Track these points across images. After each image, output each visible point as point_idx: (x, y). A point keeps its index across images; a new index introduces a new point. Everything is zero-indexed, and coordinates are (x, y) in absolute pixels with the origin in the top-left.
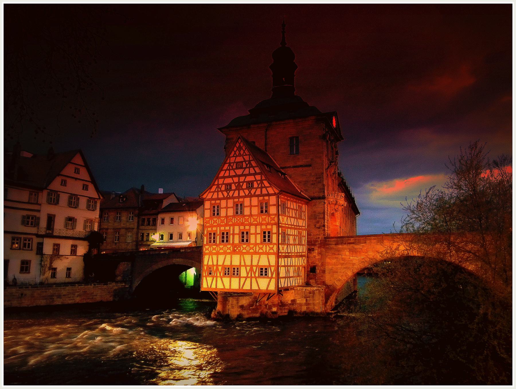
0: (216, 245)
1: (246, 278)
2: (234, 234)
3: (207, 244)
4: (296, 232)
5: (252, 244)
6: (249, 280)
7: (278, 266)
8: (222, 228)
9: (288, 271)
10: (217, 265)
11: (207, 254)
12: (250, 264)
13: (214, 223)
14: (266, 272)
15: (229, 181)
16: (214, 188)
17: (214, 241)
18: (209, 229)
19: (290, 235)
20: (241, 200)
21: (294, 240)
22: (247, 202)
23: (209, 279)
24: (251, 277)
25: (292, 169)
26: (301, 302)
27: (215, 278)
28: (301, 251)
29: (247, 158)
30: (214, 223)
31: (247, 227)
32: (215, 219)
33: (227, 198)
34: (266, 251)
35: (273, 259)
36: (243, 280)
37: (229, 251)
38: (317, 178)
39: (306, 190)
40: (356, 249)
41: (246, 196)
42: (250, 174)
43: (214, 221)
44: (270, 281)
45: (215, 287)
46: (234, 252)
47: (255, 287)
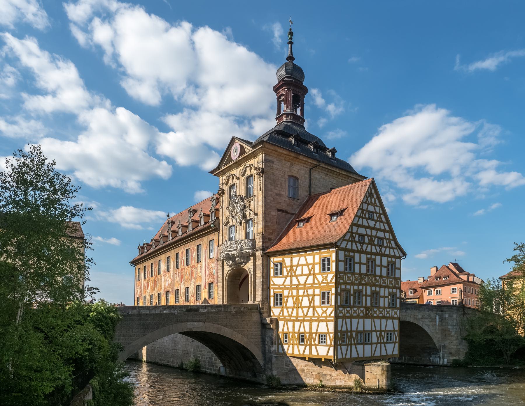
0: (350, 306)
2: (366, 295)
3: (341, 306)
5: (381, 308)
6: (379, 345)
8: (356, 287)
10: (351, 331)
12: (379, 329)
13: (348, 280)
15: (362, 231)
17: (346, 303)
18: (343, 287)
20: (373, 257)
23: (344, 348)
24: (381, 343)
27: (349, 346)
30: (348, 280)
31: (378, 289)
32: (349, 275)
36: (374, 346)
41: (377, 254)
42: (380, 230)
43: (348, 277)
46: (366, 316)
47: (384, 353)
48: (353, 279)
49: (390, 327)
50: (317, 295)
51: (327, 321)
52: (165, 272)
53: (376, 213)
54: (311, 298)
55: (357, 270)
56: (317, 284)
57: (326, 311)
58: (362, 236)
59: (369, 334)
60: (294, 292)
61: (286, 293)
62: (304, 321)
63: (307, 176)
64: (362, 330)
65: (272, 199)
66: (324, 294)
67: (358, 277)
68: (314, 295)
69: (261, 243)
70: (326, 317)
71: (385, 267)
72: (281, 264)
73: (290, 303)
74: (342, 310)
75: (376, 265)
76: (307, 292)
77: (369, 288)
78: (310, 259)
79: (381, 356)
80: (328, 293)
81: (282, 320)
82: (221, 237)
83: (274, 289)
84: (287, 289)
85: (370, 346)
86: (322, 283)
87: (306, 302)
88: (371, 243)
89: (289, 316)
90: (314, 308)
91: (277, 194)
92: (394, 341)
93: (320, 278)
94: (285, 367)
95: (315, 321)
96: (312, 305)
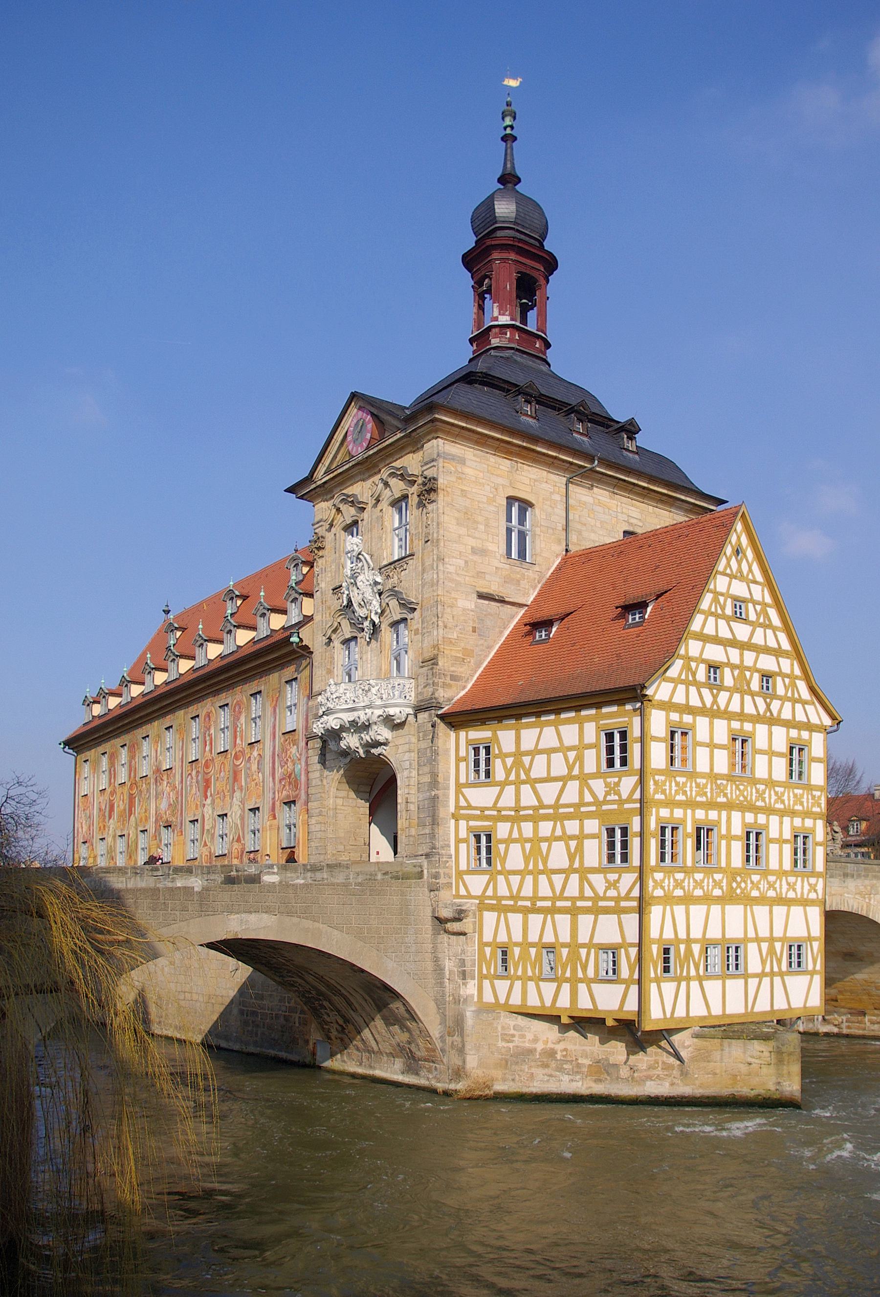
6: (766, 981)
8: (700, 814)
10: (689, 941)
11: (659, 900)
12: (767, 935)
14: (799, 956)
18: (664, 813)
23: (668, 988)
24: (772, 974)
31: (762, 819)
34: (802, 893)
36: (753, 983)
37: (717, 892)
43: (677, 784)
45: (684, 1015)
47: (780, 1004)
48: (692, 790)
49: (797, 930)
50: (593, 836)
51: (619, 911)
52: (158, 770)
53: (755, 603)
54: (573, 844)
55: (702, 766)
56: (589, 804)
57: (618, 881)
58: (714, 667)
59: (737, 948)
60: (527, 828)
61: (502, 830)
62: (553, 911)
63: (557, 497)
64: (720, 937)
65: (461, 563)
66: (611, 832)
67: (705, 786)
68: (581, 837)
69: (431, 690)
70: (618, 899)
71: (780, 755)
72: (488, 749)
73: (515, 858)
74: (663, 881)
76: (563, 827)
77: (736, 816)
78: (570, 733)
79: (772, 1011)
80: (625, 831)
81: (491, 908)
82: (318, 672)
83: (468, 818)
84: (506, 819)
85: (741, 982)
86: (605, 802)
87: (558, 856)
88: (742, 688)
89: (511, 897)
90: (584, 873)
91: (474, 551)
92: (810, 967)
93: (598, 786)
94: (501, 1044)
95: (587, 911)
96: (576, 865)
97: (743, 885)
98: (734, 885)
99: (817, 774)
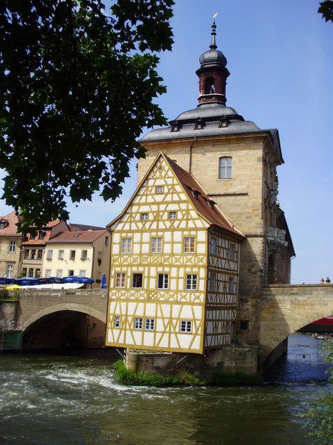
0: (126, 289)
1: (163, 333)
2: (149, 277)
4: (226, 278)
5: (173, 291)
6: (166, 336)
7: (206, 320)
9: (216, 327)
10: (126, 315)
11: (113, 300)
12: (169, 316)
13: (124, 262)
15: (144, 209)
16: (125, 219)
18: (118, 269)
19: (220, 281)
20: (160, 234)
21: (225, 287)
22: (167, 236)
23: (116, 332)
25: (223, 198)
26: (230, 365)
28: (231, 302)
29: (170, 181)
30: (124, 262)
31: (167, 270)
33: (142, 231)
34: (190, 300)
35: (199, 312)
36: (158, 336)
37: (141, 298)
38: (254, 210)
39: (240, 225)
40: (299, 301)
41: (166, 230)
42: (173, 202)
44: (194, 338)
46: (149, 300)
47: (174, 345)
48: (130, 260)
71: (178, 243)
75: (164, 243)
85: (153, 334)
97: (155, 296)
98: (151, 296)
99: (202, 249)
